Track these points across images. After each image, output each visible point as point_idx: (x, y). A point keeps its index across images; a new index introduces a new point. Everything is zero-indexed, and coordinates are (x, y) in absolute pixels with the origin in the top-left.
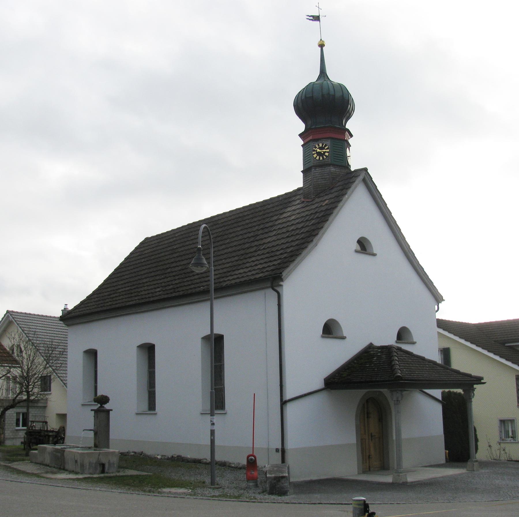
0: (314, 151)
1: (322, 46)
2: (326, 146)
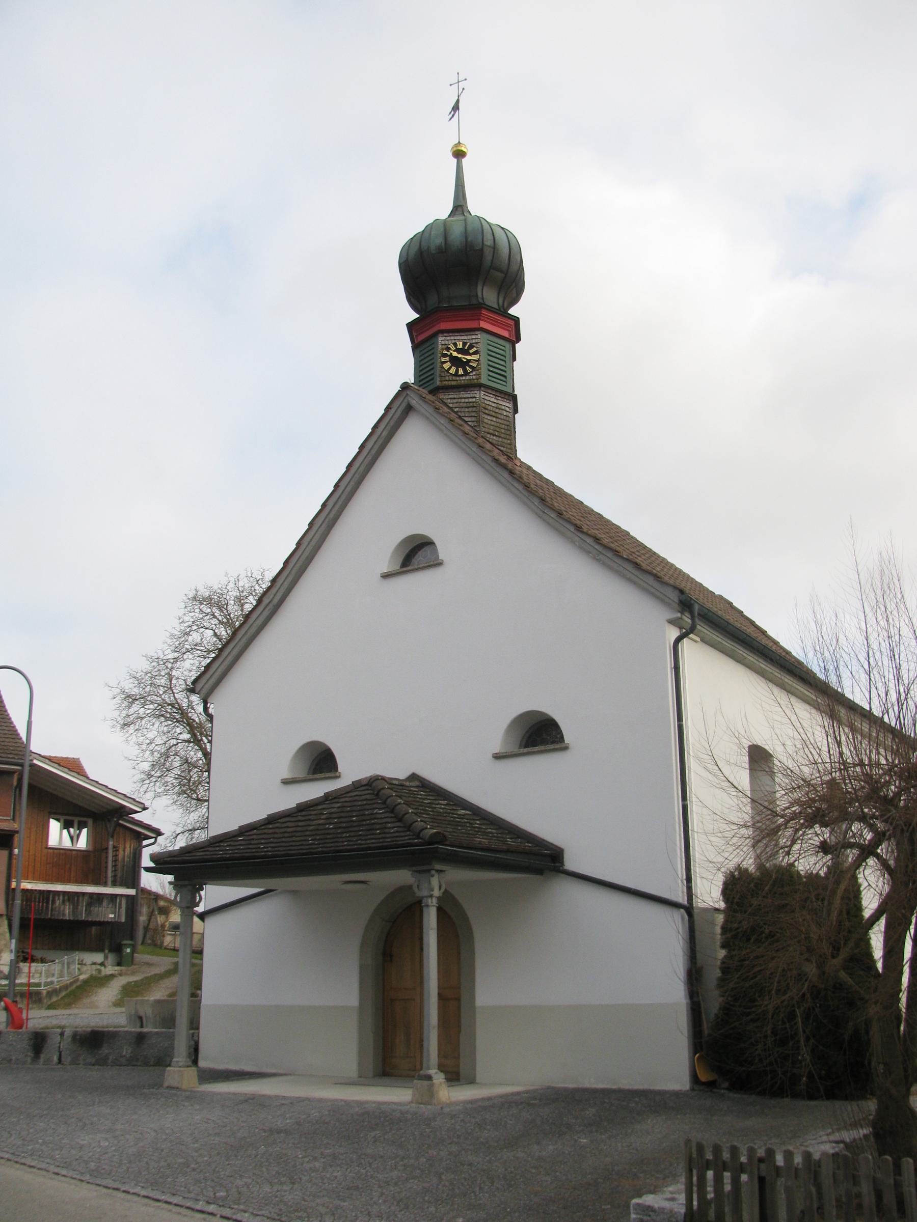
0: (445, 355)
1: (459, 154)
2: (471, 347)
